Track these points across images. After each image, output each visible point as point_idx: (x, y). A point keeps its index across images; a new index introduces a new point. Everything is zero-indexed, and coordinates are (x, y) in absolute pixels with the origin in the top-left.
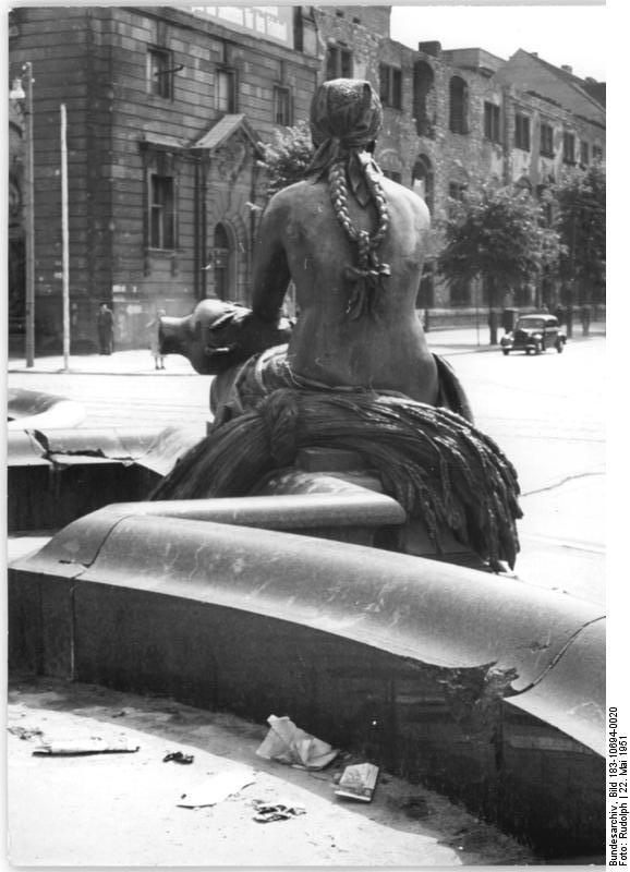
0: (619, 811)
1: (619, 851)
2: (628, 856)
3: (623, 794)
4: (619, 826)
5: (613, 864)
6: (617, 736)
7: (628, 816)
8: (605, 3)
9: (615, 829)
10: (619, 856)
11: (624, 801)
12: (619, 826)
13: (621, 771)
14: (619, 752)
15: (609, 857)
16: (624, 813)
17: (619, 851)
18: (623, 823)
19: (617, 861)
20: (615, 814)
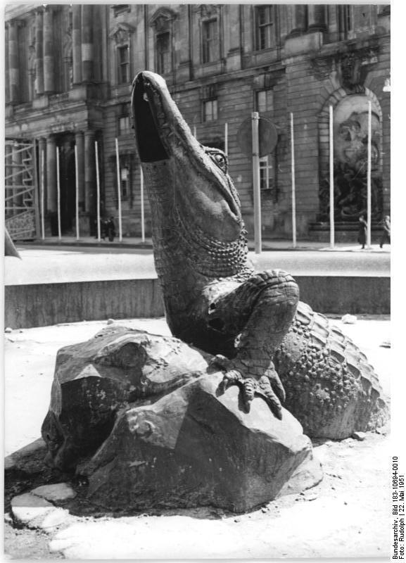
0: (399, 523)
1: (399, 549)
2: (405, 552)
3: (402, 512)
4: (399, 534)
5: (395, 557)
6: (397, 475)
7: (405, 527)
9: (396, 535)
10: (399, 553)
11: (402, 517)
12: (399, 534)
13: (400, 498)
14: (399, 485)
16: (402, 525)
17: (399, 549)
18: (402, 531)
19: (398, 556)
20: (396, 525)
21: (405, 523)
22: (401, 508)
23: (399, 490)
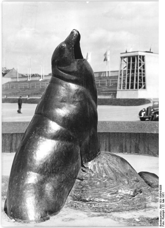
0: (162, 212)
1: (162, 222)
2: (164, 224)
3: (163, 208)
4: (162, 216)
5: (161, 226)
6: (161, 193)
7: (164, 213)
8: (158, 1)
9: (161, 217)
10: (162, 224)
11: (164, 209)
12: (162, 216)
14: (162, 197)
15: (159, 224)
16: (163, 213)
17: (162, 222)
18: (163, 215)
19: (162, 225)
21: (164, 212)
22: (163, 206)
23: (162, 198)
